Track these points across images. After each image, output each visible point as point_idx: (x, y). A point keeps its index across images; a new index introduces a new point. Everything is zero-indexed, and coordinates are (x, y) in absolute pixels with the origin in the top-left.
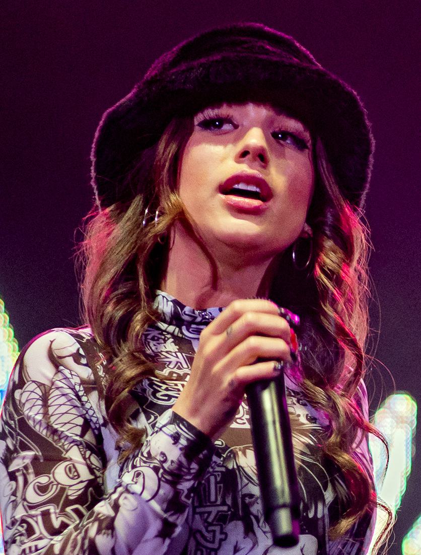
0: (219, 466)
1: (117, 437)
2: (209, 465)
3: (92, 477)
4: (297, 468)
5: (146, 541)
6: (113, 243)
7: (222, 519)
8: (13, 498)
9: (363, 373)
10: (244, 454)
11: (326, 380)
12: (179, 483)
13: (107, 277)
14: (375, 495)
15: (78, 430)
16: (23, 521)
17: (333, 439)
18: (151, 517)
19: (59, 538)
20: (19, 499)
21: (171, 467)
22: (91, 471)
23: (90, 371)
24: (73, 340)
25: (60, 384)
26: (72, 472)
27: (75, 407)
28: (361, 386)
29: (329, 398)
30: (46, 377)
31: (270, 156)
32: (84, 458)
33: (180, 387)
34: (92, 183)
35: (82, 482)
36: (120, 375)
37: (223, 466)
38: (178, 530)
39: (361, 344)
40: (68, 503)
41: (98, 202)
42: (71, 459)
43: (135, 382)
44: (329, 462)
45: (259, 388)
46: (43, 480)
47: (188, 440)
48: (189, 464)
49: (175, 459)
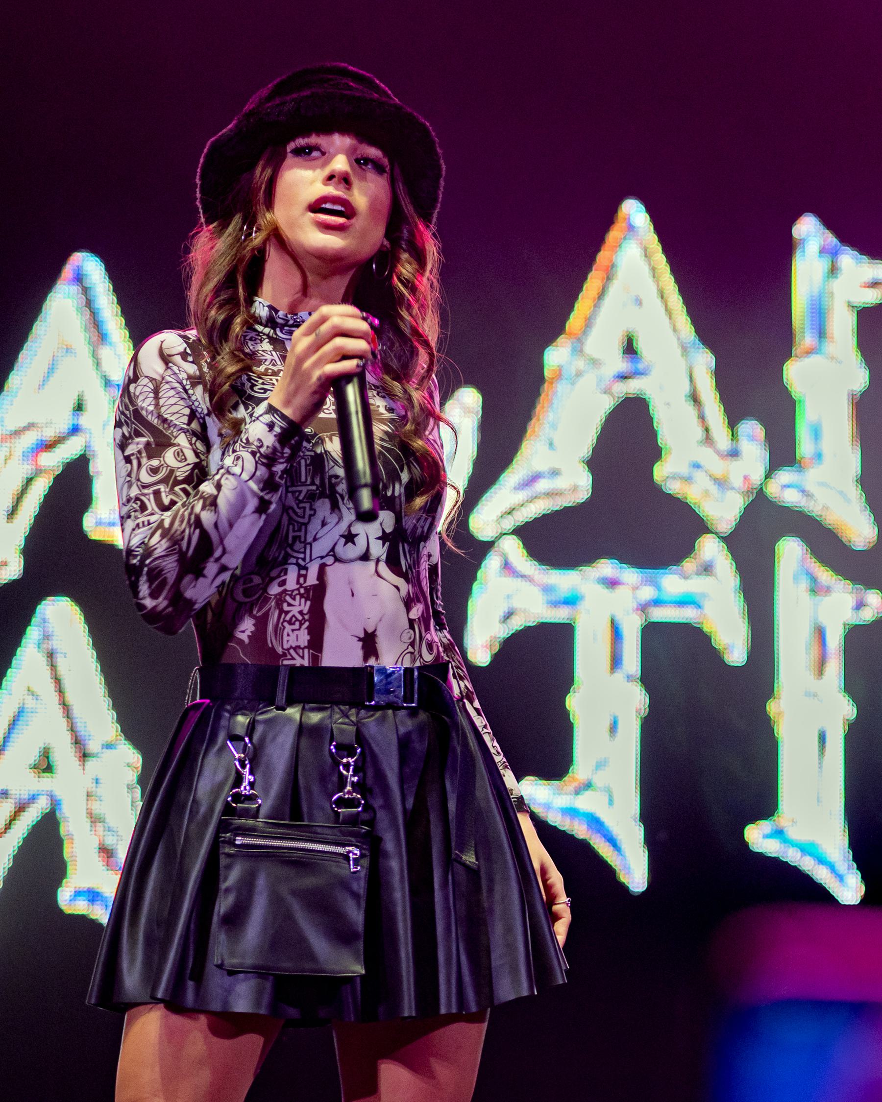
0: (308, 450)
1: (219, 425)
2: (300, 450)
3: (198, 460)
4: (377, 452)
5: (245, 516)
6: (216, 256)
7: (312, 497)
8: (128, 479)
9: (435, 369)
10: (331, 440)
11: (402, 376)
12: (273, 465)
13: (211, 285)
14: (445, 476)
15: (185, 419)
16: (137, 499)
17: (409, 427)
18: (249, 495)
19: (169, 513)
20: (133, 480)
21: (267, 452)
22: (197, 455)
23: (195, 367)
24: (181, 340)
25: (169, 379)
26: (180, 456)
27: (183, 399)
28: (433, 381)
29: (405, 391)
30: (157, 373)
31: (354, 180)
32: (191, 444)
33: (274, 381)
34: (198, 203)
35: (188, 464)
36: (222, 371)
37: (312, 451)
38: (273, 507)
39: (433, 344)
40: (177, 483)
41: (203, 220)
42: (179, 445)
43: (235, 377)
44: (405, 448)
45: (343, 383)
46: (155, 463)
47: (281, 427)
48: (283, 449)
49: (270, 445)
